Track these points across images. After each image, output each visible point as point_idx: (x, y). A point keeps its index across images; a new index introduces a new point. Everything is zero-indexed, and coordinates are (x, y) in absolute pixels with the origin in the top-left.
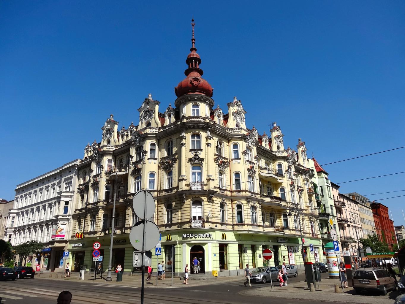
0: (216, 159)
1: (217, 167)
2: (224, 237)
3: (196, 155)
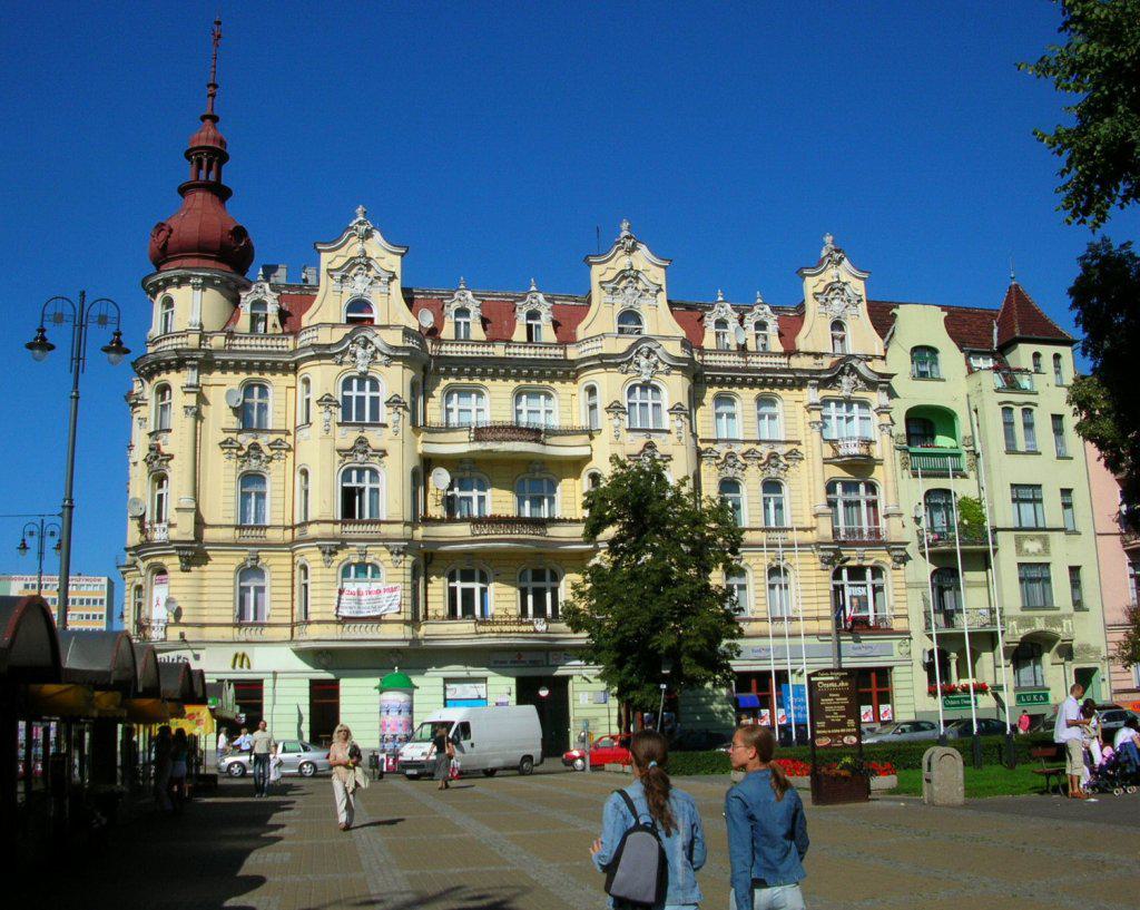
0: (225, 442)
1: (229, 467)
2: (241, 659)
3: (151, 449)
